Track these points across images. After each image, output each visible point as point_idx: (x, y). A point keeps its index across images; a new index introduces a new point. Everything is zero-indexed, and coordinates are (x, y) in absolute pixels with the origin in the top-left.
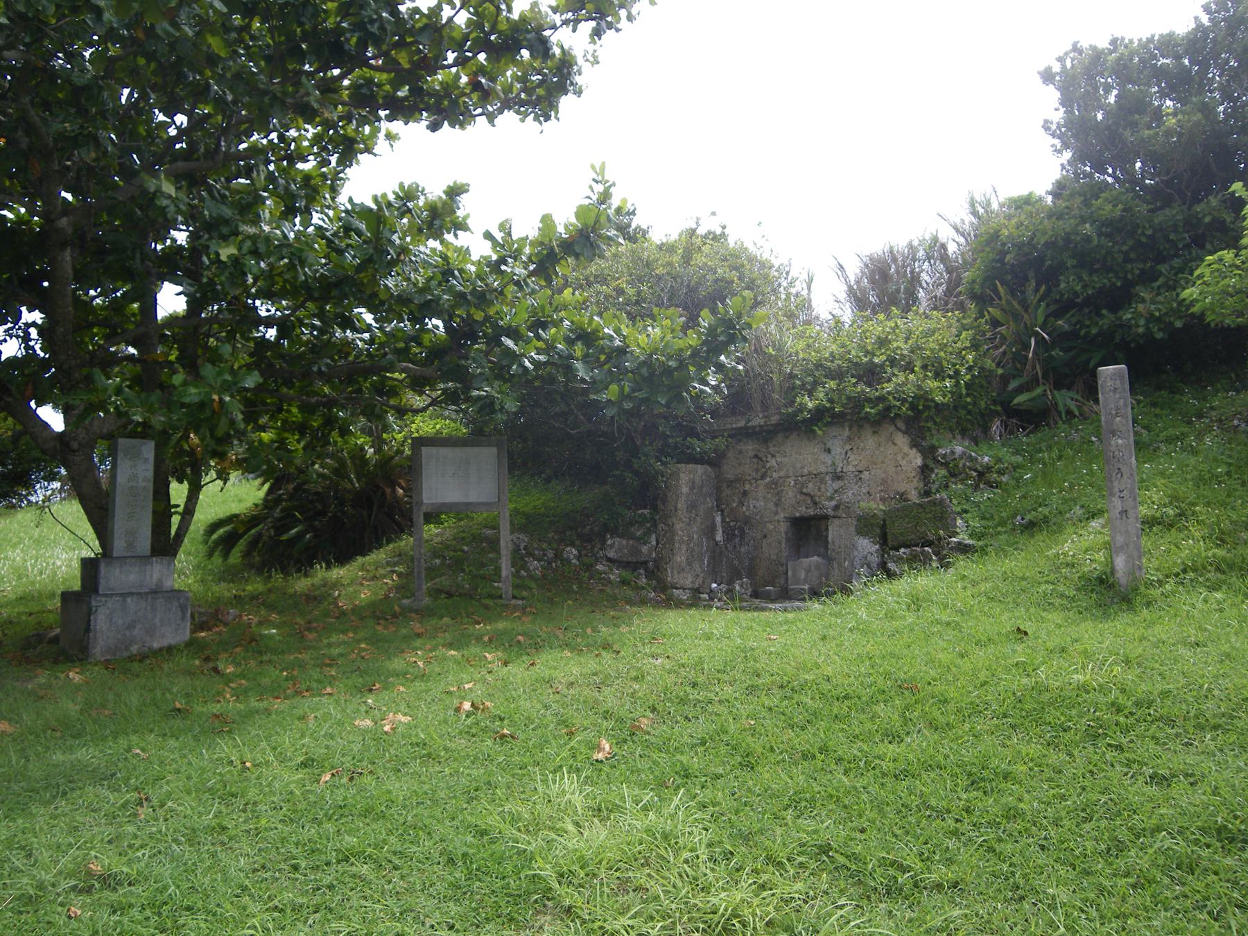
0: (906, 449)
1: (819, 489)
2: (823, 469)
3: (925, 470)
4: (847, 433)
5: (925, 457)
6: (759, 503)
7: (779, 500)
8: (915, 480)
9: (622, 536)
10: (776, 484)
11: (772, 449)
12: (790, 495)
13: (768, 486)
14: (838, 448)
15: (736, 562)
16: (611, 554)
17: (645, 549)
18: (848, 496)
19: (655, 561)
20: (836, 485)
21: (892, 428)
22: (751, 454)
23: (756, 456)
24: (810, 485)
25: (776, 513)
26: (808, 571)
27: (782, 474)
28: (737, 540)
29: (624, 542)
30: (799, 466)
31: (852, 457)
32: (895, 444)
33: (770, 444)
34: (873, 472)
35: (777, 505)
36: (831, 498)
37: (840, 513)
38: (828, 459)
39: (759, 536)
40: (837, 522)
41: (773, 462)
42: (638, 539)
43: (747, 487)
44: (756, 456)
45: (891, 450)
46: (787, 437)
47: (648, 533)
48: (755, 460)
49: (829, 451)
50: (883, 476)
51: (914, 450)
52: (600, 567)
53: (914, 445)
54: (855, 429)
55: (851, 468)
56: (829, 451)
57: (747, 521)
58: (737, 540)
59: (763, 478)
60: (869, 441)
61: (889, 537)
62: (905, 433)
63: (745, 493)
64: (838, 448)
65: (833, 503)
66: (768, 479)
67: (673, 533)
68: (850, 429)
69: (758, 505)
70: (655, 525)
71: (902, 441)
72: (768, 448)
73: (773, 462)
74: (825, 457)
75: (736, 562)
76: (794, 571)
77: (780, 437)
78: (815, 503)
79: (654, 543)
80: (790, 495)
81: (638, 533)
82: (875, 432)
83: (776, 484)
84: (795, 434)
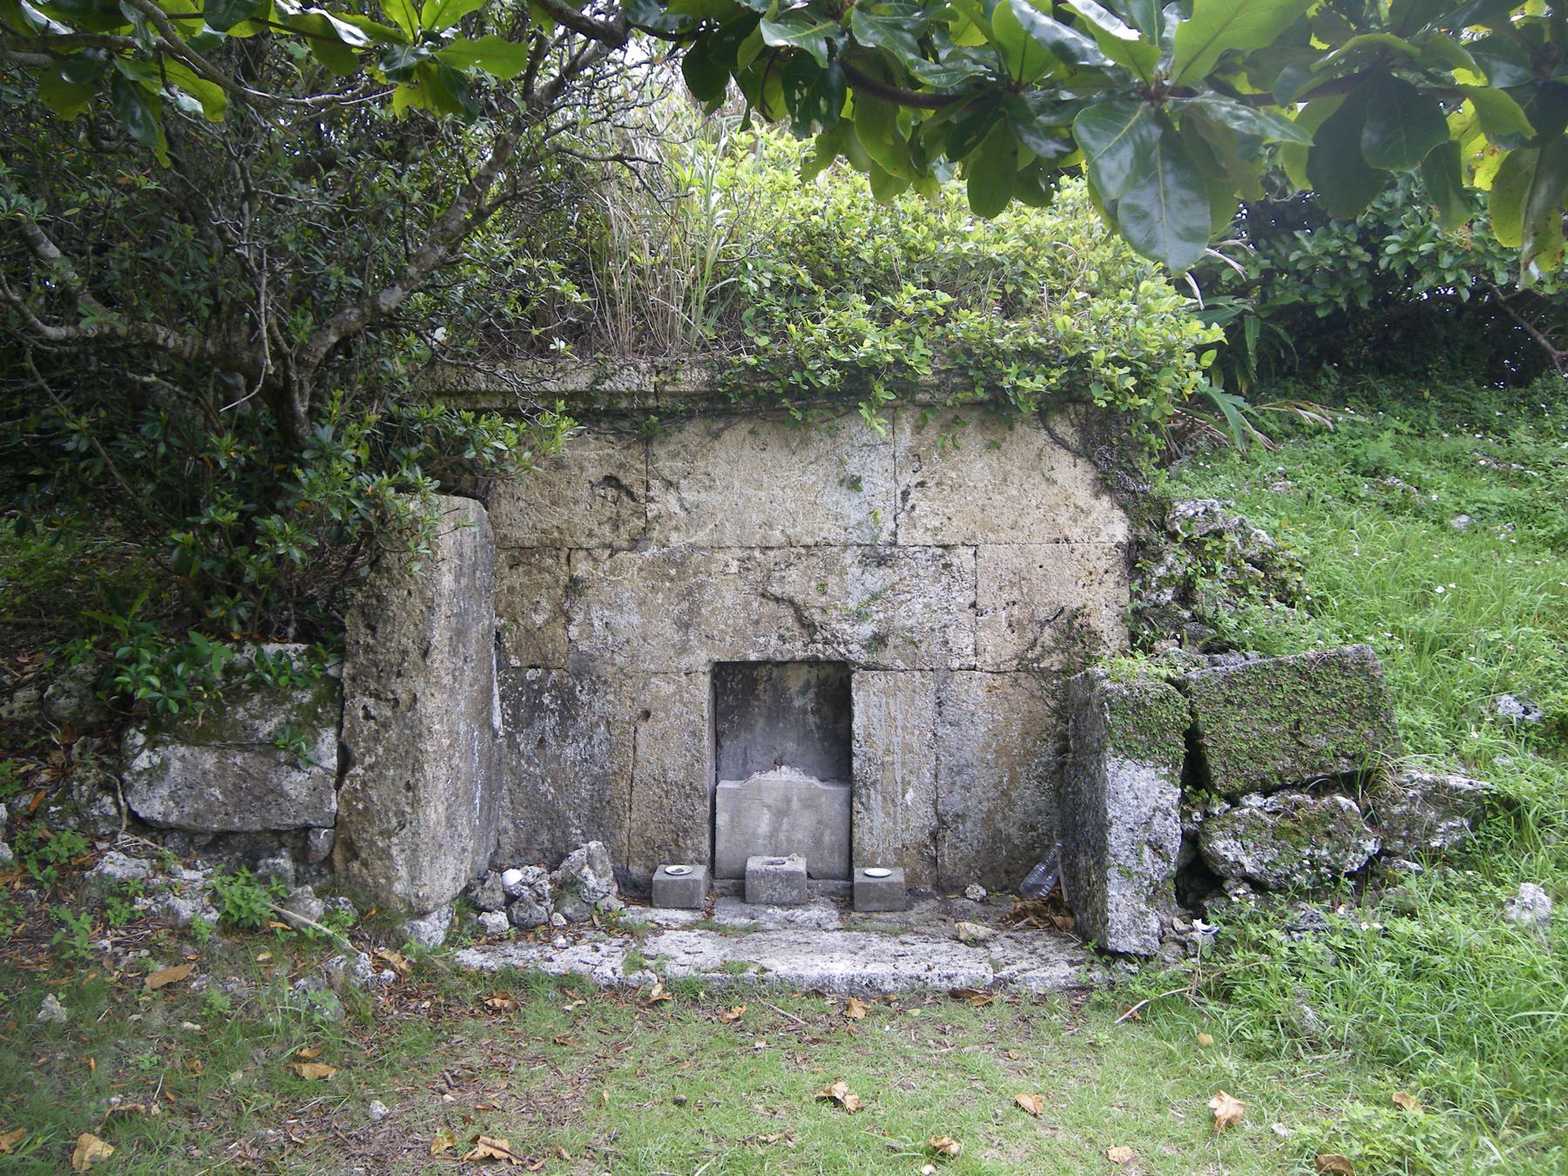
0: (1083, 496)
1: (822, 589)
2: (831, 531)
3: (1135, 556)
4: (906, 438)
5: (1135, 519)
6: (624, 615)
7: (694, 611)
8: (1110, 579)
9: (199, 739)
10: (680, 565)
11: (665, 465)
12: (727, 599)
13: (654, 571)
14: (880, 482)
15: (547, 788)
16: (153, 806)
17: (296, 784)
18: (913, 612)
19: (338, 823)
20: (876, 579)
21: (1041, 438)
22: (595, 473)
23: (611, 481)
24: (793, 574)
25: (683, 649)
26: (781, 813)
27: (701, 537)
28: (551, 722)
29: (209, 760)
30: (757, 518)
31: (923, 507)
32: (1051, 482)
33: (660, 451)
34: (986, 552)
35: (684, 626)
36: (860, 616)
37: (886, 656)
38: (852, 509)
39: (625, 712)
40: (878, 681)
41: (669, 502)
42: (269, 747)
43: (582, 568)
44: (611, 481)
45: (1039, 493)
46: (716, 436)
47: (308, 721)
48: (611, 493)
49: (854, 484)
50: (1019, 563)
51: (1105, 501)
52: (116, 865)
53: (1104, 485)
54: (931, 433)
55: (920, 537)
56: (854, 484)
57: (583, 668)
58: (551, 722)
59: (635, 544)
60: (974, 463)
61: (1214, 762)
62: (1077, 454)
63: (575, 586)
64: (880, 482)
65: (867, 630)
66: (652, 552)
67: (416, 734)
68: (918, 429)
69: (620, 621)
70: (334, 694)
71: (1073, 475)
72: (649, 458)
73: (669, 502)
74: (836, 497)
75: (547, 788)
76: (736, 815)
77: (692, 433)
78: (809, 627)
79: (332, 762)
80: (727, 599)
81: (266, 728)
82: (993, 446)
83: (680, 565)
84: (743, 428)
